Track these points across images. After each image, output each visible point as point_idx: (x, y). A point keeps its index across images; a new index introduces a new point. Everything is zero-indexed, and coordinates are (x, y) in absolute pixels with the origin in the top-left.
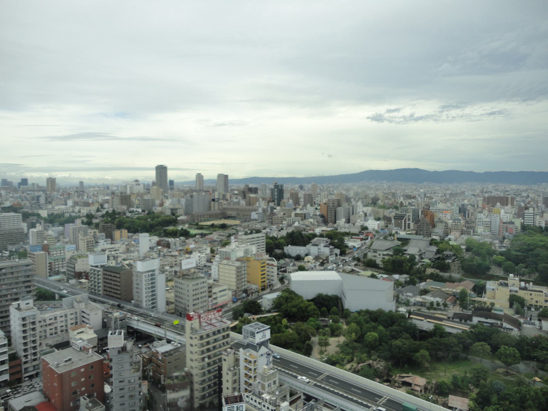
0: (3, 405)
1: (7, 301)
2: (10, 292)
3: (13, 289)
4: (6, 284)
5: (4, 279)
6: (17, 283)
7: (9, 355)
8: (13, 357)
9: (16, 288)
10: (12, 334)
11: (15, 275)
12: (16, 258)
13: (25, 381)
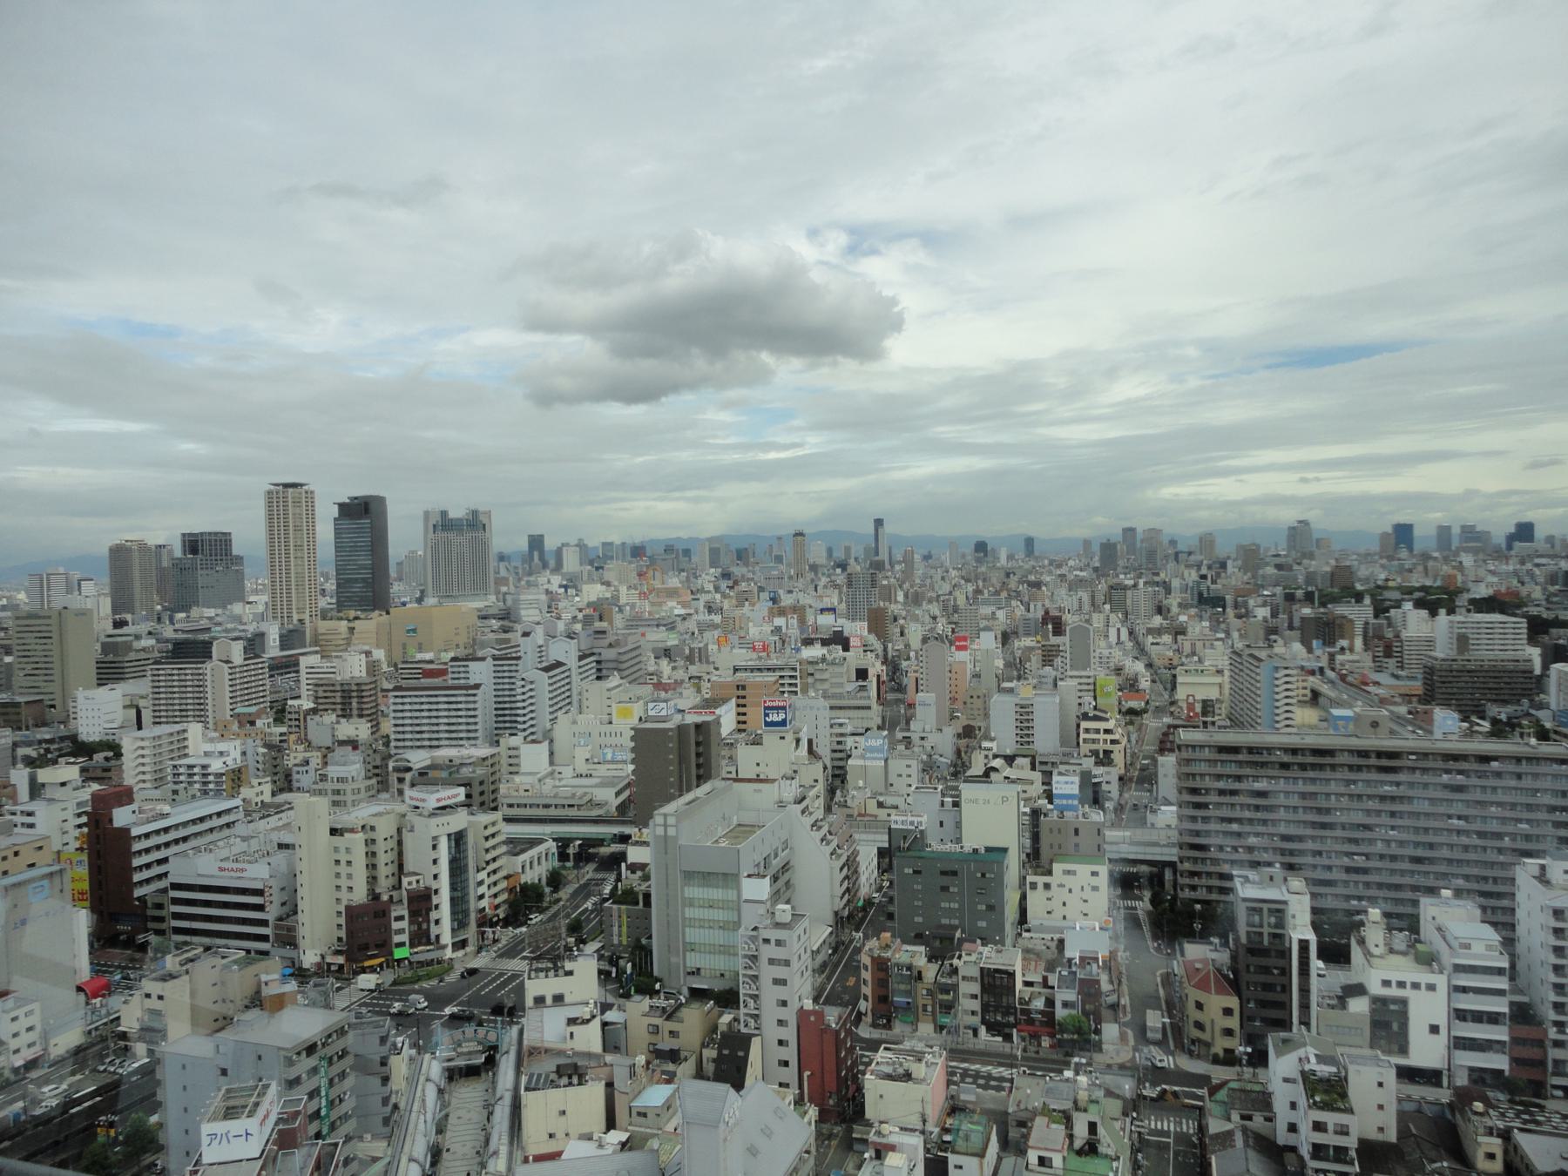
0: (1499, 1136)
1: (1500, 851)
2: (1510, 828)
3: (1520, 821)
4: (1499, 804)
5: (1494, 789)
6: (1529, 807)
7: (1512, 1004)
8: (1522, 1014)
9: (1528, 821)
10: (1520, 948)
11: (1527, 782)
12: (1529, 735)
13: (1553, 1097)
